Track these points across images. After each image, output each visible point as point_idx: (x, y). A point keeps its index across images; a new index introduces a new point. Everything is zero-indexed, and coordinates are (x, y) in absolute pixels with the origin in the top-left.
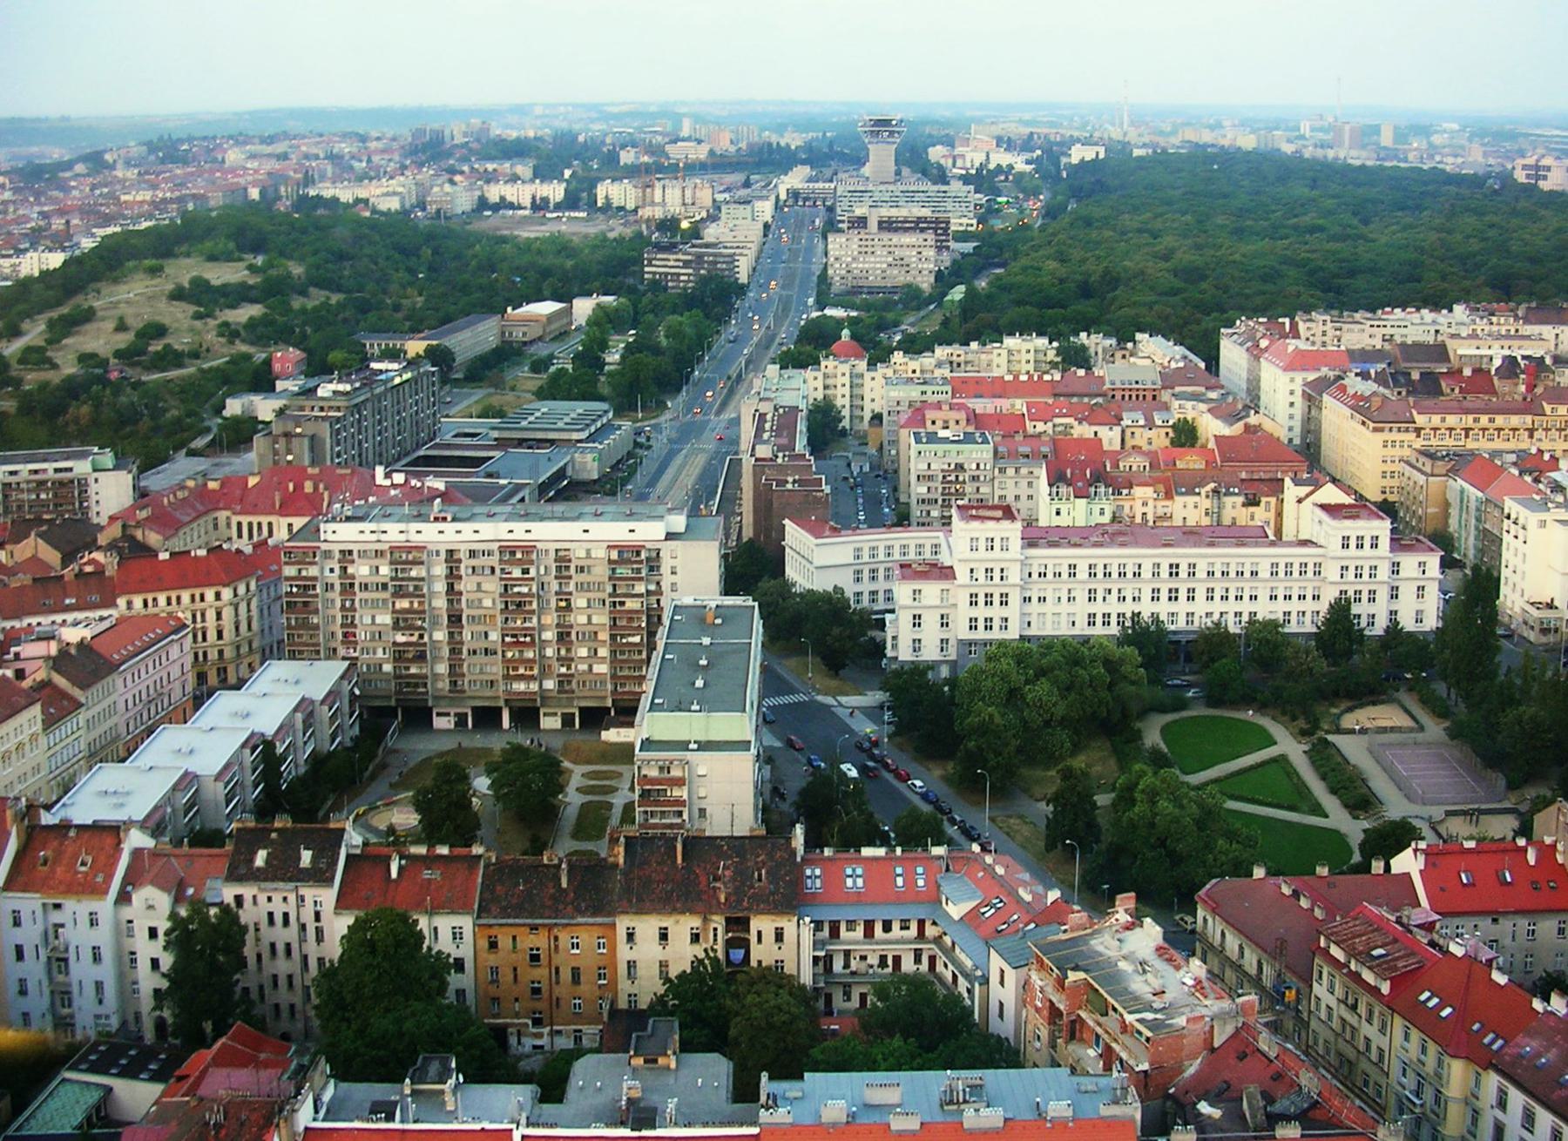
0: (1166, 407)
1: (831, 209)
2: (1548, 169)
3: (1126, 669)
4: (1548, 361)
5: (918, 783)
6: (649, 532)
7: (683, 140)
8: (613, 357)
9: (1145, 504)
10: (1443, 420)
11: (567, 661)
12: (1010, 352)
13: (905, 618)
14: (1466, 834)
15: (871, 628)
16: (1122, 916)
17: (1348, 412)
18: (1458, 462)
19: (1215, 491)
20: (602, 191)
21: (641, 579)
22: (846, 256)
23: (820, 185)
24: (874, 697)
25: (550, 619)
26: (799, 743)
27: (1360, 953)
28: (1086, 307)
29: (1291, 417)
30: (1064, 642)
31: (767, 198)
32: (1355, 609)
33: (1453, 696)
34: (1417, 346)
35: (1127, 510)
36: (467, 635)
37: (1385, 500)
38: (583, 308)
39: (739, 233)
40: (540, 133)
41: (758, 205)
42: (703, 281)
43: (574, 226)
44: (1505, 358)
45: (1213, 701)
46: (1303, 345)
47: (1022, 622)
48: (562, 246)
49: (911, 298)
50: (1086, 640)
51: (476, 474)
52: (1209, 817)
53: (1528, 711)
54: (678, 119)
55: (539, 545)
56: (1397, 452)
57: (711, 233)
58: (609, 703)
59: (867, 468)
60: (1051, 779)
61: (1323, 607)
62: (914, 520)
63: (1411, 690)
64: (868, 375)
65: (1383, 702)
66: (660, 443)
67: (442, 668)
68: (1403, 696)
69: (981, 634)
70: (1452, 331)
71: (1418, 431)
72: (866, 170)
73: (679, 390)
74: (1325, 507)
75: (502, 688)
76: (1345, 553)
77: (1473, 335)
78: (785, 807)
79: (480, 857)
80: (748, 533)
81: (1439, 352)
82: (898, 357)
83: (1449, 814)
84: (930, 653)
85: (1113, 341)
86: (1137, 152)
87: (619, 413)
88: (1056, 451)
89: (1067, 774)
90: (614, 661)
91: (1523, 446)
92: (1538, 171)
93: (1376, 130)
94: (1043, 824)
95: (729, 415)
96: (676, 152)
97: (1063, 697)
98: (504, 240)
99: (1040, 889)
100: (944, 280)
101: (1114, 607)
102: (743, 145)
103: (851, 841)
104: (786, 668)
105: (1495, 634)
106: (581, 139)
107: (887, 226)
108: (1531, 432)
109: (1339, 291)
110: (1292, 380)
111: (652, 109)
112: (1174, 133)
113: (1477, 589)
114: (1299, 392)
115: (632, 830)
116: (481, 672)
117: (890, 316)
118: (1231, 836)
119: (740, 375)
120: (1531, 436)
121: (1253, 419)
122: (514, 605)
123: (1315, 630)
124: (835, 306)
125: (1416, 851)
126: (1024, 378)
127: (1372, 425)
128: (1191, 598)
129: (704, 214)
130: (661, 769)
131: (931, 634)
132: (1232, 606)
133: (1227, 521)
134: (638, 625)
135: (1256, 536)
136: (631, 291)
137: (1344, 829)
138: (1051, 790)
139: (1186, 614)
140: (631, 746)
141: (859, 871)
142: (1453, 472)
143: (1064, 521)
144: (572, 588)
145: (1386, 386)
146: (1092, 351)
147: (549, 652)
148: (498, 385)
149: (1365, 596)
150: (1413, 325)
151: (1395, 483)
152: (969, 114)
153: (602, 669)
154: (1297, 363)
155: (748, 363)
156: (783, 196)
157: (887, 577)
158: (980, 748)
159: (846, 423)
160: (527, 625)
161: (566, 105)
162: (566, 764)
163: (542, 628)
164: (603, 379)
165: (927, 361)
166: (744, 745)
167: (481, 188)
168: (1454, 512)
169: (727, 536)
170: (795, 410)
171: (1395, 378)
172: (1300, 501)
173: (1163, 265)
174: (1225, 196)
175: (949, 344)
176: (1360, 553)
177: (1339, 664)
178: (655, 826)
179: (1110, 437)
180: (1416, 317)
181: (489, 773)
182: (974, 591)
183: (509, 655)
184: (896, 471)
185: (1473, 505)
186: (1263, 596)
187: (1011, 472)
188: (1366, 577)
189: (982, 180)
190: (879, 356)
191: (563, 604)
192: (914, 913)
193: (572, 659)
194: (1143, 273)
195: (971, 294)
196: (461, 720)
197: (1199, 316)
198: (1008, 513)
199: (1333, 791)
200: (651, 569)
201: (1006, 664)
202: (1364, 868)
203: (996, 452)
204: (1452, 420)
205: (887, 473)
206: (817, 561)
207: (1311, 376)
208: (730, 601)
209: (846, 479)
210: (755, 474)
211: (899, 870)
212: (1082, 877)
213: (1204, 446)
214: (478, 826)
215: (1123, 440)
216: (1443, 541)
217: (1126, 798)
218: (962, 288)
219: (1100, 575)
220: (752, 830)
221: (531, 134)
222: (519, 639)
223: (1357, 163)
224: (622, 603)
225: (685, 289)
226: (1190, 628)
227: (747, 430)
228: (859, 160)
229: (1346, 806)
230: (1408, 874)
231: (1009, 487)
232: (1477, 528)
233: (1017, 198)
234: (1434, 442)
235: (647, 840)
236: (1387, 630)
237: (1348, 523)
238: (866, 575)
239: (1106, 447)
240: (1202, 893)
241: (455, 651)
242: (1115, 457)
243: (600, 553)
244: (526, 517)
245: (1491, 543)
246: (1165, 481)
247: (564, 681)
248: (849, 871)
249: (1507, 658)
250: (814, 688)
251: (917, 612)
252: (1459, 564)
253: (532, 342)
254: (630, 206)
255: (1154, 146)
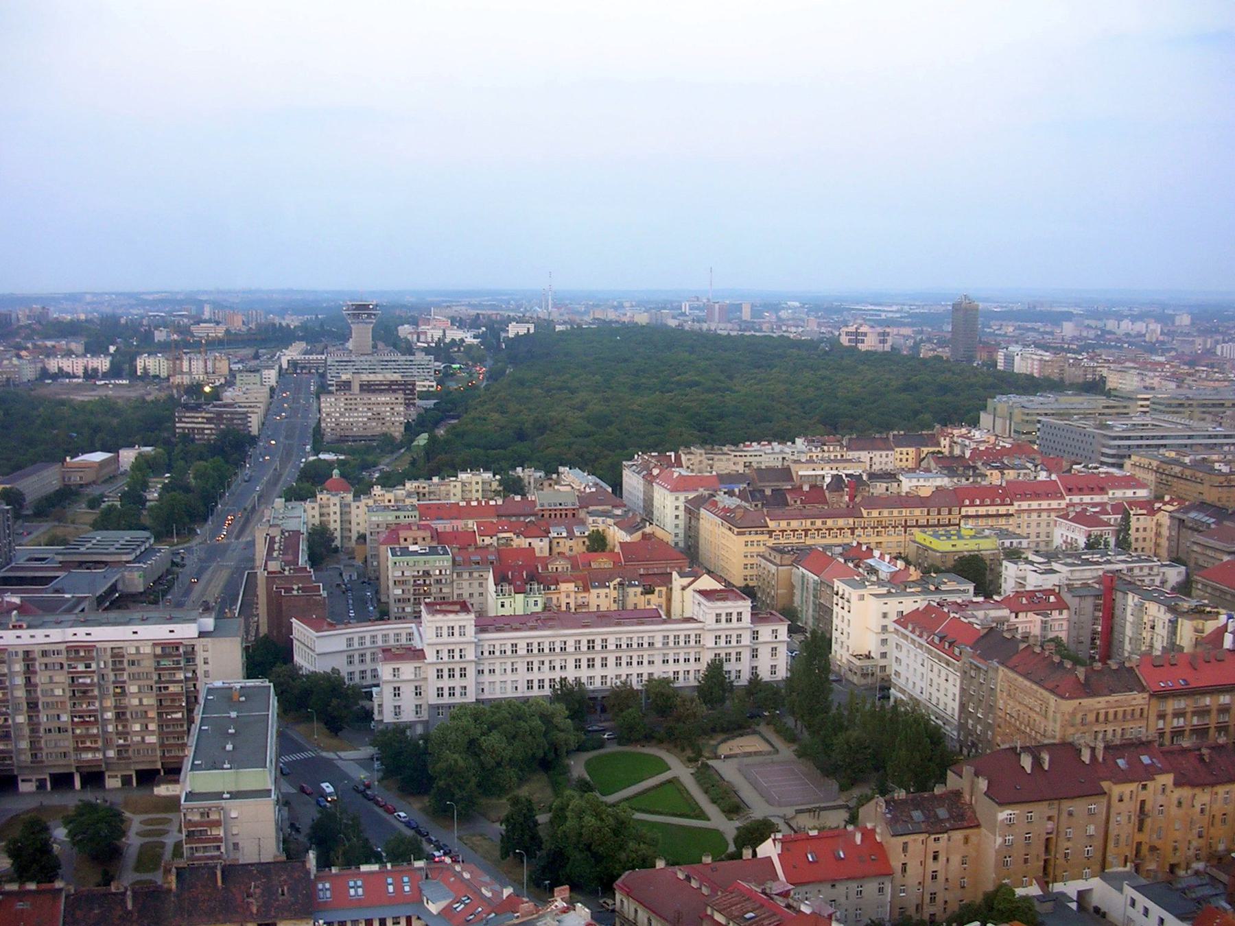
0: (583, 523)
1: (323, 376)
2: (865, 334)
3: (558, 720)
4: (865, 477)
5: (402, 814)
6: (186, 631)
7: (205, 321)
8: (153, 495)
9: (568, 596)
10: (789, 524)
11: (124, 734)
12: (463, 484)
13: (388, 691)
14: (811, 825)
15: (362, 699)
16: (560, 903)
17: (719, 521)
18: (800, 555)
19: (621, 584)
20: (139, 364)
21: (180, 669)
22: (334, 412)
23: (314, 357)
24: (367, 751)
25: (109, 703)
26: (309, 790)
27: (736, 917)
28: (522, 448)
29: (677, 526)
30: (509, 702)
31: (272, 368)
32: (726, 667)
33: (799, 726)
34: (770, 470)
35: (555, 601)
36: (43, 718)
37: (747, 586)
38: (128, 456)
39: (251, 395)
40: (90, 316)
41: (265, 372)
42: (224, 434)
43: (119, 390)
44: (833, 476)
45: (621, 741)
46: (684, 473)
47: (477, 689)
48: (108, 406)
49: (387, 444)
50: (526, 700)
51: (45, 591)
52: (620, 828)
53: (854, 733)
54: (200, 304)
55: (98, 645)
56: (755, 549)
57: (229, 395)
58: (159, 766)
59: (355, 577)
60: (503, 806)
61: (703, 666)
62: (392, 615)
63: (768, 724)
64: (354, 505)
65: (748, 734)
66: (192, 562)
67: (24, 745)
68: (762, 728)
69: (446, 700)
70: (795, 458)
71: (770, 533)
72: (350, 345)
73: (206, 520)
74: (704, 593)
75: (73, 757)
76: (719, 626)
77: (811, 461)
78: (302, 838)
79: (60, 890)
80: (264, 630)
81: (786, 473)
82: (377, 490)
83: (798, 812)
84: (408, 716)
85: (542, 474)
86: (559, 328)
87: (159, 538)
88: (500, 558)
89: (515, 801)
90: (162, 734)
91: (846, 541)
92: (857, 336)
93: (739, 308)
94: (498, 839)
95: (245, 539)
96: (200, 331)
97: (510, 744)
98: (62, 403)
99: (497, 887)
100: (411, 430)
101: (547, 675)
102: (253, 326)
103: (352, 861)
104: (297, 732)
105: (828, 679)
106: (123, 321)
107: (367, 388)
108: (853, 530)
109: (711, 430)
110: (677, 499)
111: (179, 297)
112: (586, 313)
113: (814, 647)
114: (682, 508)
115: (182, 863)
116: (56, 746)
117: (370, 458)
118: (640, 839)
119: (254, 507)
120: (853, 534)
121: (648, 529)
122: (80, 693)
123: (697, 684)
124: (328, 451)
125: (774, 840)
126: (474, 503)
127: (736, 530)
128: (604, 665)
129: (222, 381)
130: (202, 814)
131: (408, 701)
132: (635, 670)
133: (630, 606)
134: (179, 701)
135: (651, 617)
136: (167, 442)
137: (721, 828)
138: (504, 813)
139: (600, 676)
140: (178, 798)
141: (359, 883)
142: (796, 562)
143: (507, 611)
144: (125, 677)
145: (747, 501)
146: (526, 481)
147: (110, 728)
148: (60, 519)
149: (733, 657)
150: (766, 454)
151: (754, 572)
152: (429, 299)
153: (152, 739)
154: (678, 486)
155: (260, 497)
156: (285, 366)
157: (373, 660)
158: (448, 785)
159: (338, 543)
160: (92, 708)
161: (110, 294)
162: (127, 814)
163: (104, 709)
164: (145, 513)
165: (400, 492)
166: (266, 793)
167: (42, 361)
168: (797, 592)
169: (247, 632)
170: (298, 533)
171: (753, 494)
172: (683, 589)
173: (578, 414)
174: (626, 360)
175: (416, 479)
176: (729, 625)
177: (721, 705)
178: (199, 859)
179: (540, 546)
180: (768, 449)
181: (66, 825)
182: (440, 667)
183: (78, 731)
184: (378, 579)
185: (811, 586)
186: (658, 660)
187: (466, 576)
188: (734, 643)
189: (441, 351)
190: (362, 489)
191: (118, 690)
192: (403, 911)
193: (128, 733)
194: (563, 420)
195: (433, 440)
196: (41, 785)
197: (606, 452)
198: (464, 607)
199: (714, 801)
200: (188, 661)
201: (466, 722)
202: (737, 856)
203: (454, 560)
204: (795, 524)
205: (371, 580)
206: (318, 649)
207: (691, 496)
208: (251, 683)
209: (338, 585)
210: (267, 583)
211: (390, 880)
212: (530, 877)
213: (612, 551)
214: (59, 866)
215: (550, 549)
216: (789, 614)
217: (559, 815)
218: (425, 435)
219: (535, 651)
220: (275, 856)
221: (83, 317)
222: (83, 720)
223: (724, 333)
224: (166, 688)
225: (209, 440)
226: (604, 687)
227: (261, 550)
228: (344, 337)
229: (724, 811)
230: (770, 858)
231: (465, 587)
232: (814, 603)
233: (466, 364)
234: (782, 541)
235: (192, 869)
236: (750, 681)
237: (719, 604)
238: (356, 658)
239: (538, 554)
240: (619, 881)
241: (34, 730)
242: (545, 562)
243: (147, 650)
244: (86, 623)
245: (825, 613)
246: (583, 579)
247: (121, 750)
248: (352, 884)
249: (838, 697)
250: (320, 747)
251: (397, 685)
252: (801, 630)
253: (88, 485)
254: (164, 374)
255: (571, 322)
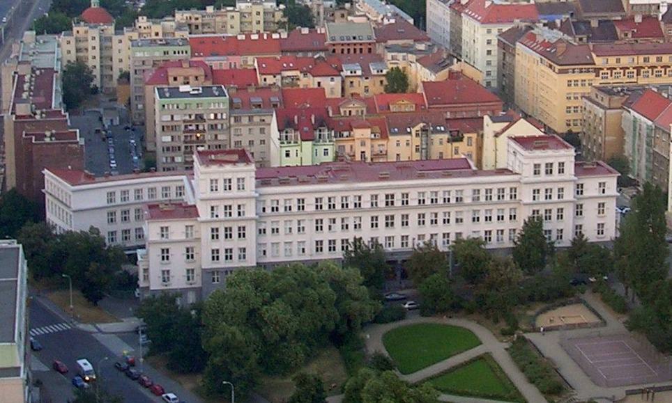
0: (380, 59)
3: (351, 287)
9: (363, 144)
10: (618, 61)
12: (242, 15)
13: (154, 253)
15: (126, 262)
17: (537, 57)
18: (631, 97)
19: (424, 130)
24: (130, 323)
26: (64, 367)
29: (489, 63)
30: (295, 266)
32: (546, 226)
33: (630, 294)
35: (348, 149)
37: (570, 132)
45: (424, 311)
47: (258, 251)
50: (314, 264)
56: (579, 90)
59: (116, 122)
61: (519, 225)
62: (160, 166)
63: (594, 291)
64: (116, 39)
65: (571, 303)
68: (588, 296)
69: (222, 263)
71: (597, 71)
74: (519, 140)
76: (537, 178)
82: (142, 21)
84: (178, 282)
89: (302, 381)
101: (338, 235)
104: (51, 301)
105: (663, 240)
110: (489, 31)
114: (495, 42)
121: (456, 67)
123: (512, 245)
126: (255, 37)
127: (557, 68)
128: (405, 224)
131: (178, 265)
132: (441, 229)
133: (435, 156)
139: (399, 236)
142: (627, 105)
143: (292, 161)
145: (570, 34)
146: (315, 11)
149: (554, 215)
151: (578, 116)
155: (7, 30)
157: (138, 218)
158: (225, 362)
159: (97, 82)
165: (169, 24)
166: (14, 371)
170: (51, 71)
172: (497, 135)
175: (188, 9)
176: (549, 178)
179: (331, 86)
182: (215, 226)
184: (143, 124)
185: (644, 132)
186: (467, 218)
187: (245, 120)
188: (555, 198)
198: (243, 157)
199: (531, 381)
201: (245, 289)
204: (625, 61)
205: (136, 125)
207: (505, 28)
209: (98, 131)
210: (15, 129)
213: (414, 92)
215: (343, 89)
216: (619, 164)
219: (326, 207)
226: (405, 249)
229: (543, 392)
231: (244, 134)
232: (647, 152)
234: (611, 80)
236: (574, 242)
237: (538, 153)
238: (119, 216)
239: (328, 95)
242: (337, 104)
245: (659, 163)
250: (76, 319)
